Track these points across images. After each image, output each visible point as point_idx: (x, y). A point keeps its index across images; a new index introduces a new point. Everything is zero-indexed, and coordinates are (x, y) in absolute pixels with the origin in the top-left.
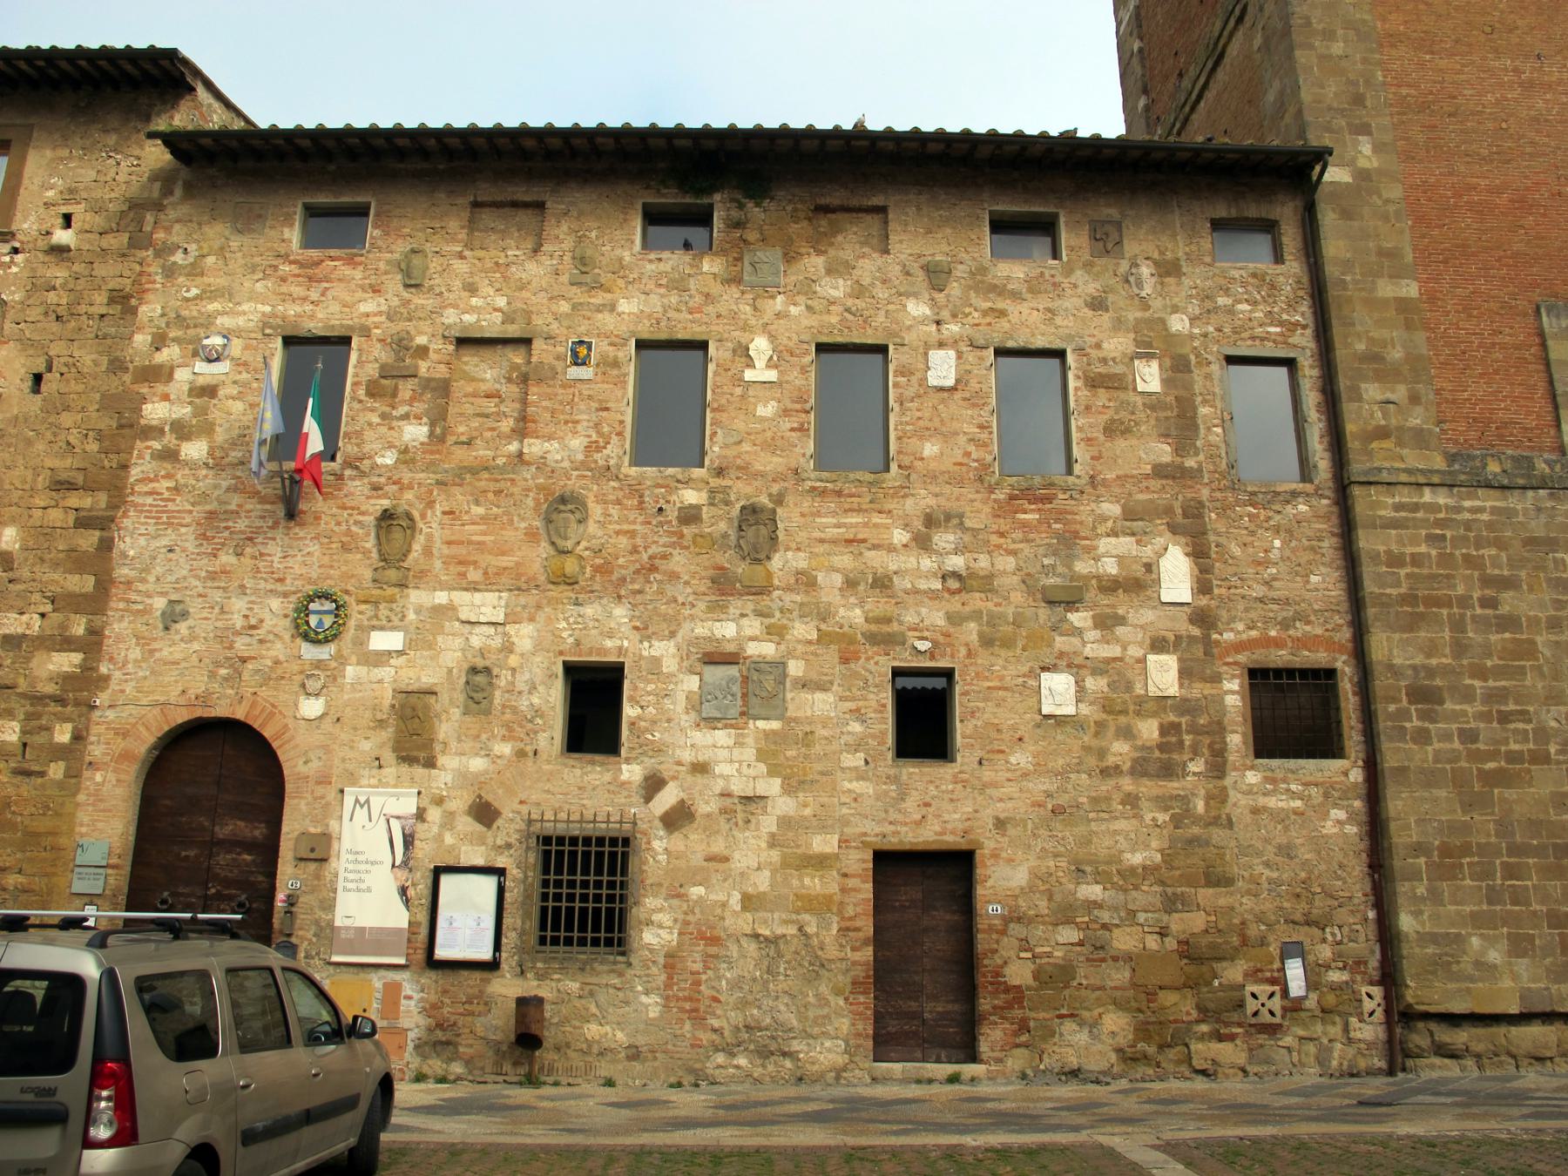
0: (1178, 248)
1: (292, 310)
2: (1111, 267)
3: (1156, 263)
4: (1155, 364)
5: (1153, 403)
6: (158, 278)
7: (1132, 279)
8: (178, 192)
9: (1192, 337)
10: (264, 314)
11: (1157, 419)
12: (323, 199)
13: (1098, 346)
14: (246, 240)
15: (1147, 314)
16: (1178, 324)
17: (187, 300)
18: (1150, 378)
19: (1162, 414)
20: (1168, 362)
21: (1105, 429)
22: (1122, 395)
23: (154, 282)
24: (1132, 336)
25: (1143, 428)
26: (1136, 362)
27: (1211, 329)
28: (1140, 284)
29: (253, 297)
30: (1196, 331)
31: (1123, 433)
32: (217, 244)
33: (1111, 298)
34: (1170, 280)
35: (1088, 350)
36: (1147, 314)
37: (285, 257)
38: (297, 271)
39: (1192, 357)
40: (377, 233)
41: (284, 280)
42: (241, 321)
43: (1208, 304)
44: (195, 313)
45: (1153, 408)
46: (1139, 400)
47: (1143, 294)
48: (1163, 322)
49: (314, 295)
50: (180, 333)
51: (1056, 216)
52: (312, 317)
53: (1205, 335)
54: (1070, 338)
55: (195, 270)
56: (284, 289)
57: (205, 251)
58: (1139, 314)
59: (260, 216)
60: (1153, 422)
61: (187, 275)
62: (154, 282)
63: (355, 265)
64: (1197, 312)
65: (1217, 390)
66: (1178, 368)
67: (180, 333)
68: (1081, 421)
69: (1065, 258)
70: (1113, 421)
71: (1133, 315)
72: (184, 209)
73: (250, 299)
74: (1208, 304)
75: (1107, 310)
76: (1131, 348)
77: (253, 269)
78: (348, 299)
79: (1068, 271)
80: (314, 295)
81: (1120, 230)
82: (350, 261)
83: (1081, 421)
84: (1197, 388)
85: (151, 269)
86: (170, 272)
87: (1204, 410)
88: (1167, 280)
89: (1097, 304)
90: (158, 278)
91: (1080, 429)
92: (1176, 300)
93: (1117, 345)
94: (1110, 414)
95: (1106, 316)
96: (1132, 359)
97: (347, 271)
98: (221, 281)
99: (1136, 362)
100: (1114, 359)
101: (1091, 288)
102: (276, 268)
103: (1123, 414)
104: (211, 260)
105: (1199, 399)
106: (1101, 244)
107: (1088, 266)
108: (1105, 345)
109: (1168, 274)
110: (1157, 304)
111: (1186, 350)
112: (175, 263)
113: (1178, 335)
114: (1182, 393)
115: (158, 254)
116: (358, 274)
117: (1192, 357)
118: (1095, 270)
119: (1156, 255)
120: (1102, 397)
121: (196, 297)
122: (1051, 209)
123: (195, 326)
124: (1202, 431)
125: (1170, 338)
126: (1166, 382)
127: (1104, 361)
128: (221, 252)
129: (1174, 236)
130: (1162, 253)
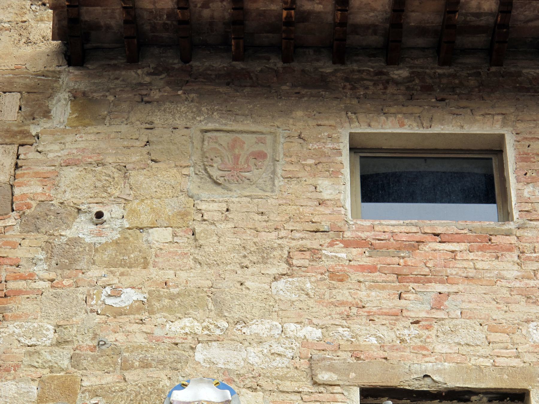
1: (371, 337)
6: (40, 270)
8: (61, 110)
10: (305, 342)
12: (395, 127)
14: (237, 198)
17: (119, 313)
23: (31, 277)
29: (271, 308)
32: (171, 206)
37: (336, 233)
38: (366, 261)
40: (527, 191)
41: (337, 277)
42: (254, 356)
44: (140, 339)
49: (419, 310)
50: (109, 379)
52: (423, 349)
55: (126, 256)
56: (343, 293)
57: (145, 220)
59: (260, 156)
61: (111, 264)
62: (31, 277)
63: (499, 252)
67: (109, 379)
72: (87, 140)
73: (267, 313)
77: (264, 255)
78: (498, 315)
80: (417, 305)
82: (485, 241)
85: (20, 253)
86: (66, 258)
90: (40, 270)
97: (484, 262)
98: (194, 278)
102: (315, 254)
104: (160, 236)
112: (75, 241)
115: (31, 224)
116: (509, 268)
121: (139, 307)
123: (145, 365)
128: (186, 223)
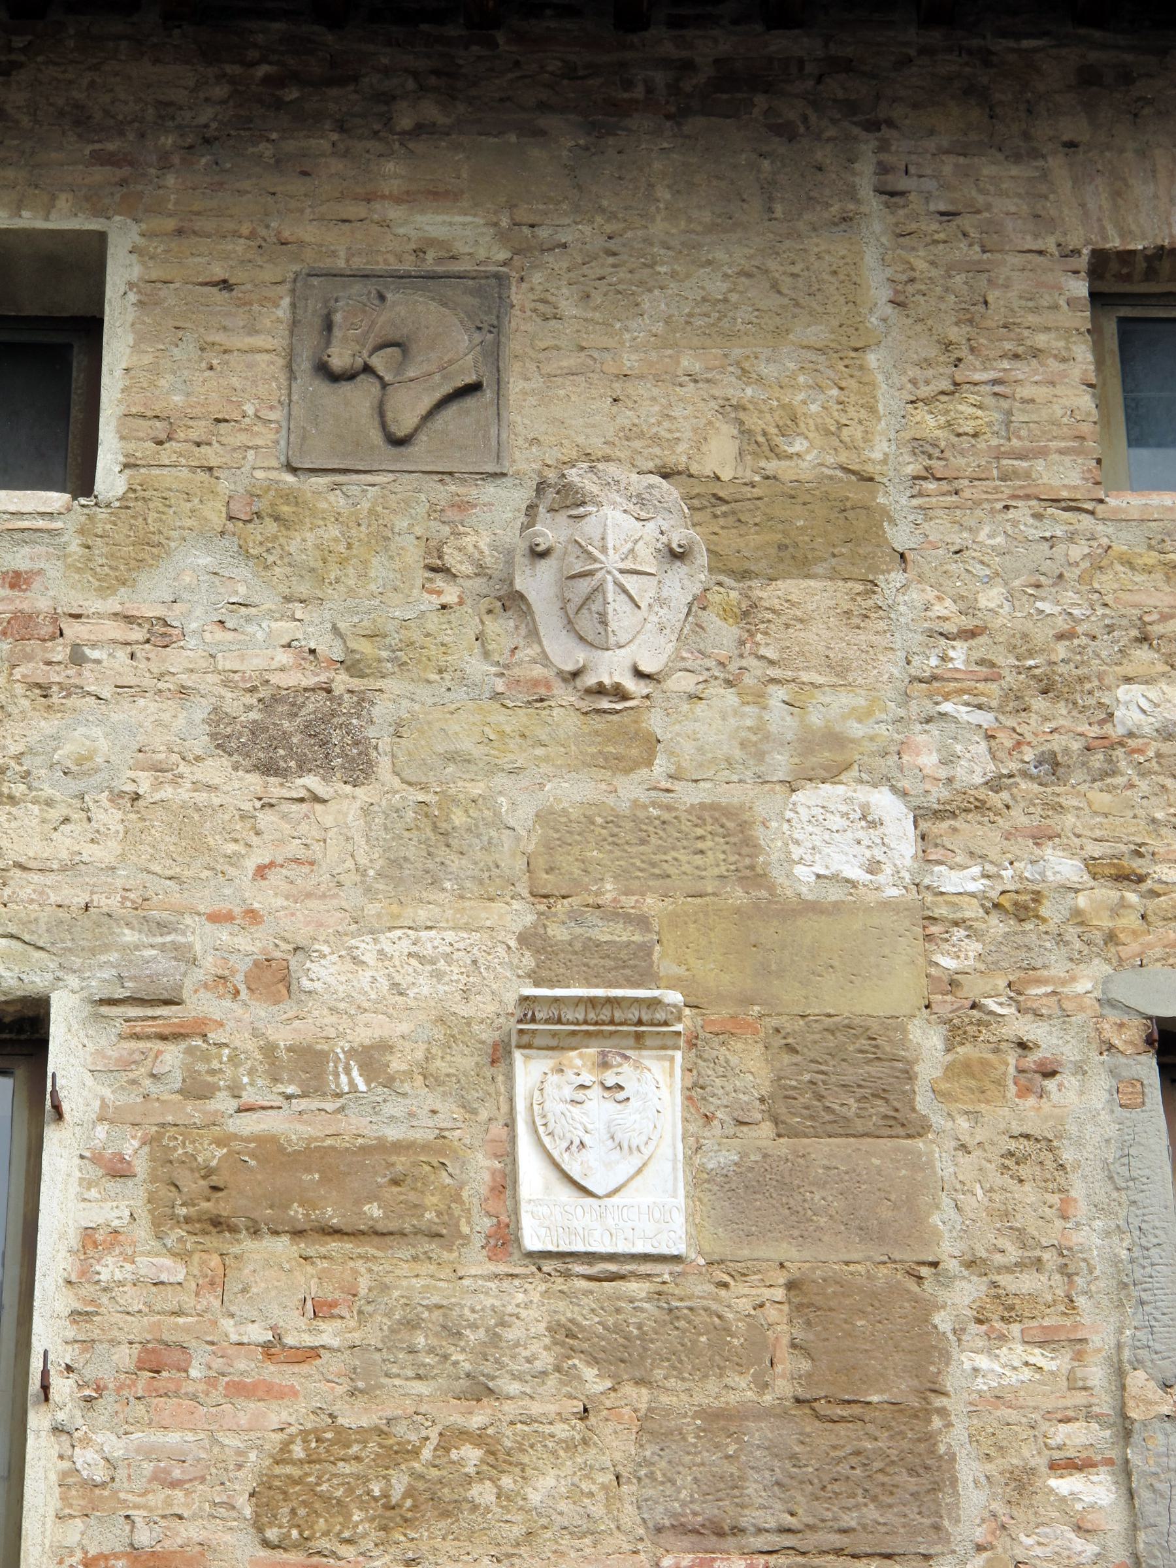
0: (872, 413)
2: (410, 530)
3: (710, 500)
4: (656, 1085)
5: (624, 1319)
7: (537, 584)
9: (931, 920)
11: (650, 1427)
13: (275, 978)
15: (630, 790)
16: (838, 842)
18: (618, 1161)
19: (683, 1397)
20: (751, 1070)
21: (266, 1496)
22: (410, 1278)
24: (518, 915)
25: (545, 1486)
26: (528, 1071)
27: (1062, 867)
28: (584, 612)
30: (961, 881)
31: (393, 1516)
33: (393, 698)
34: (813, 594)
35: (201, 1004)
36: (630, 790)
39: (927, 1043)
43: (1054, 726)
45: (624, 1355)
46: (530, 1307)
47: (611, 668)
48: (735, 830)
51: (85, 261)
53: (1022, 908)
54: (86, 926)
58: (573, 791)
60: (616, 1444)
64: (975, 767)
65: (1090, 1237)
66: (824, 1097)
68: (104, 1445)
69: (109, 478)
70: (328, 1441)
71: (542, 788)
74: (1054, 726)
75: (359, 769)
76: (509, 986)
79: (138, 546)
81: (492, 328)
83: (104, 1445)
84: (948, 1231)
87: (986, 1368)
88: (770, 594)
89: (298, 737)
91: (86, 1495)
92: (832, 707)
93: (403, 972)
94: (308, 1398)
95: (347, 806)
96: (500, 1055)
99: (528, 1071)
100: (371, 1059)
101: (271, 646)
103: (415, 1401)
105: (966, 1293)
106: (359, 398)
107: (257, 522)
108: (324, 973)
109: (794, 559)
110: (700, 730)
111: (889, 993)
113: (836, 905)
114: (835, 1256)
117: (927, 1043)
118: (302, 543)
119: (720, 457)
120: (273, 1281)
122: (65, 218)
124: (974, 1498)
125: (765, 914)
126: (729, 1193)
127: (308, 1066)
129: (849, 349)
130: (755, 444)
